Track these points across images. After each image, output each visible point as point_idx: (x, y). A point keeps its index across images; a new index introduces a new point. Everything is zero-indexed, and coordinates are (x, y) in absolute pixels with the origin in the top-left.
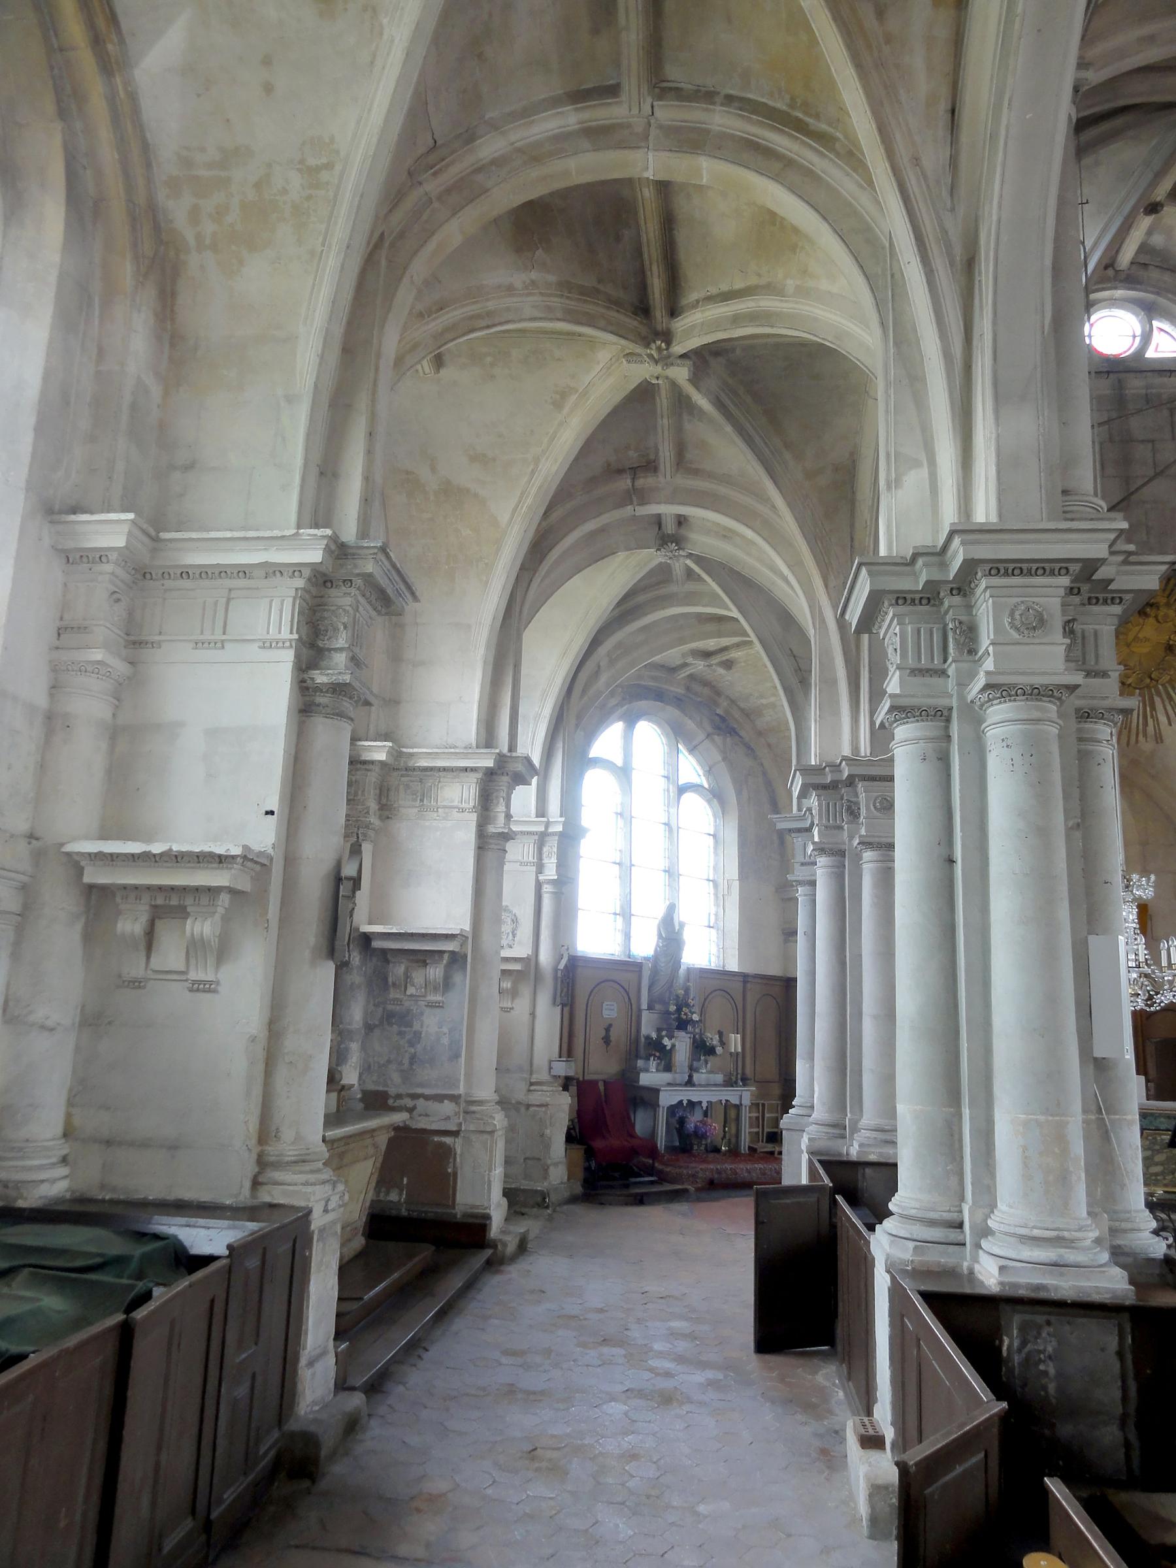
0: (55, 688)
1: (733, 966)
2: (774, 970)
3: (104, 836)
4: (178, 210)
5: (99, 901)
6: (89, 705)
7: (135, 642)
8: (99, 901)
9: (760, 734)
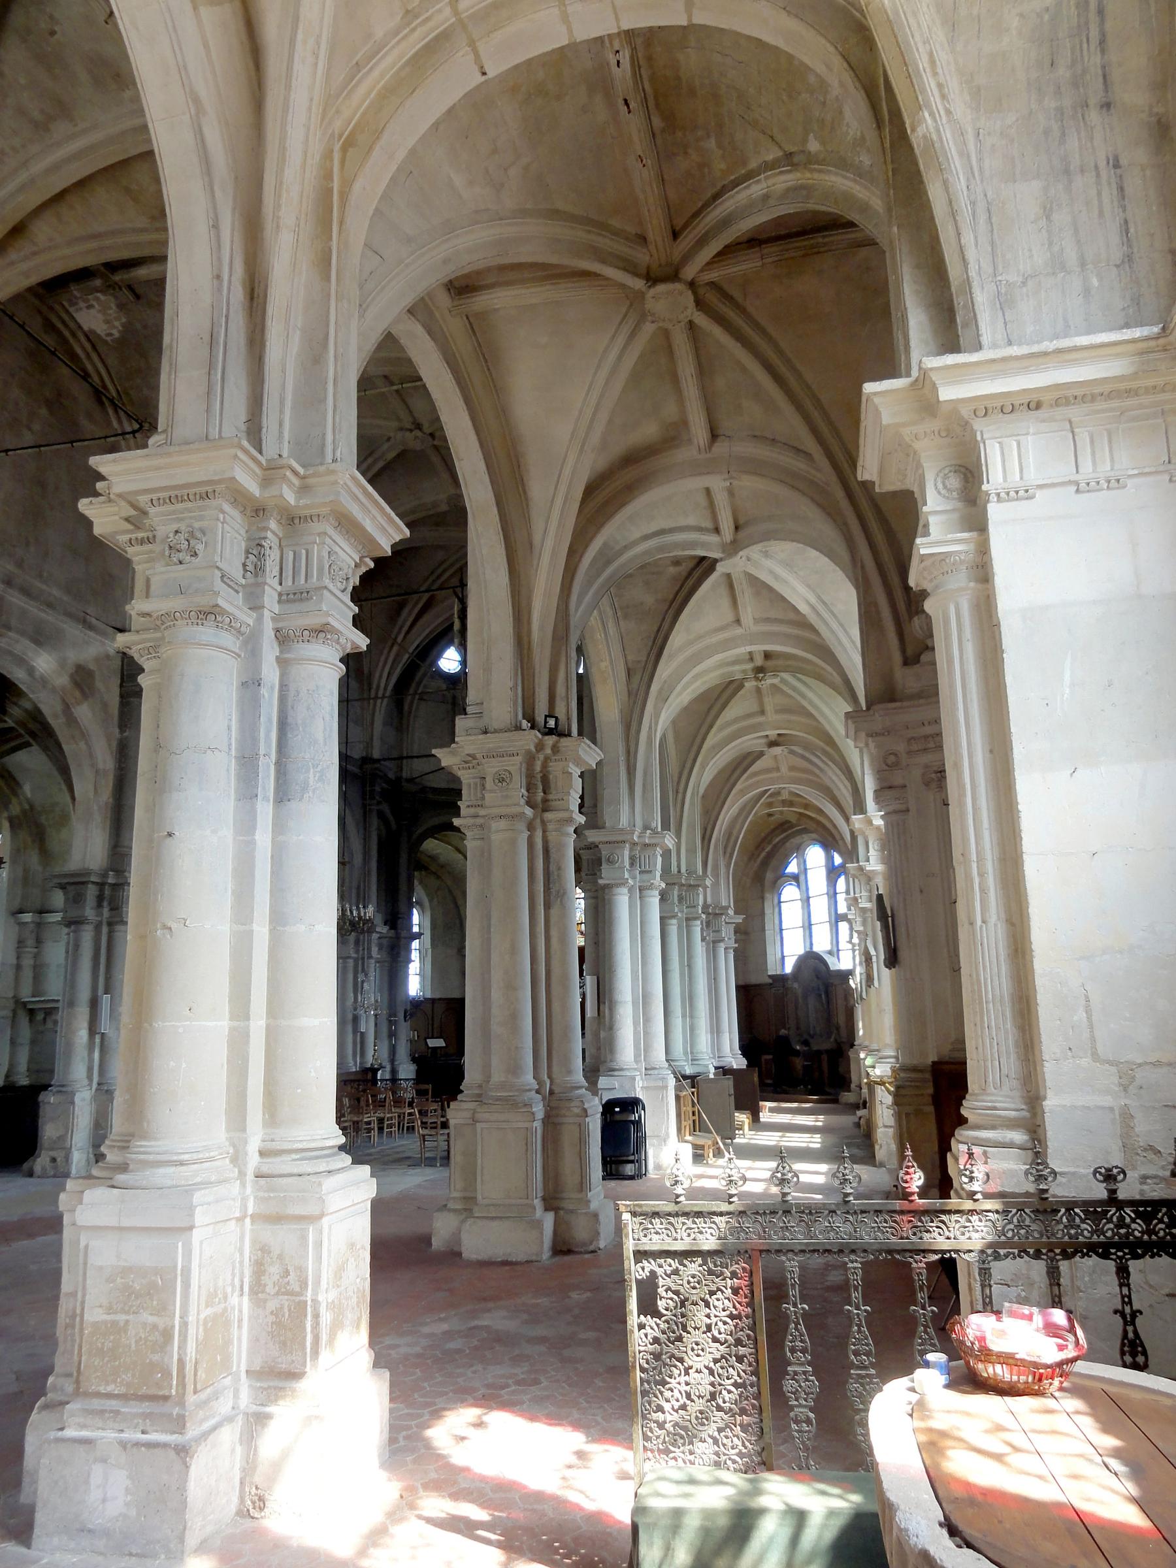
0: (18, 958)
1: (429, 995)
2: (456, 995)
3: (33, 996)
4: (43, 819)
5: (32, 1012)
6: (28, 962)
7: (39, 942)
8: (32, 1012)
9: (442, 867)
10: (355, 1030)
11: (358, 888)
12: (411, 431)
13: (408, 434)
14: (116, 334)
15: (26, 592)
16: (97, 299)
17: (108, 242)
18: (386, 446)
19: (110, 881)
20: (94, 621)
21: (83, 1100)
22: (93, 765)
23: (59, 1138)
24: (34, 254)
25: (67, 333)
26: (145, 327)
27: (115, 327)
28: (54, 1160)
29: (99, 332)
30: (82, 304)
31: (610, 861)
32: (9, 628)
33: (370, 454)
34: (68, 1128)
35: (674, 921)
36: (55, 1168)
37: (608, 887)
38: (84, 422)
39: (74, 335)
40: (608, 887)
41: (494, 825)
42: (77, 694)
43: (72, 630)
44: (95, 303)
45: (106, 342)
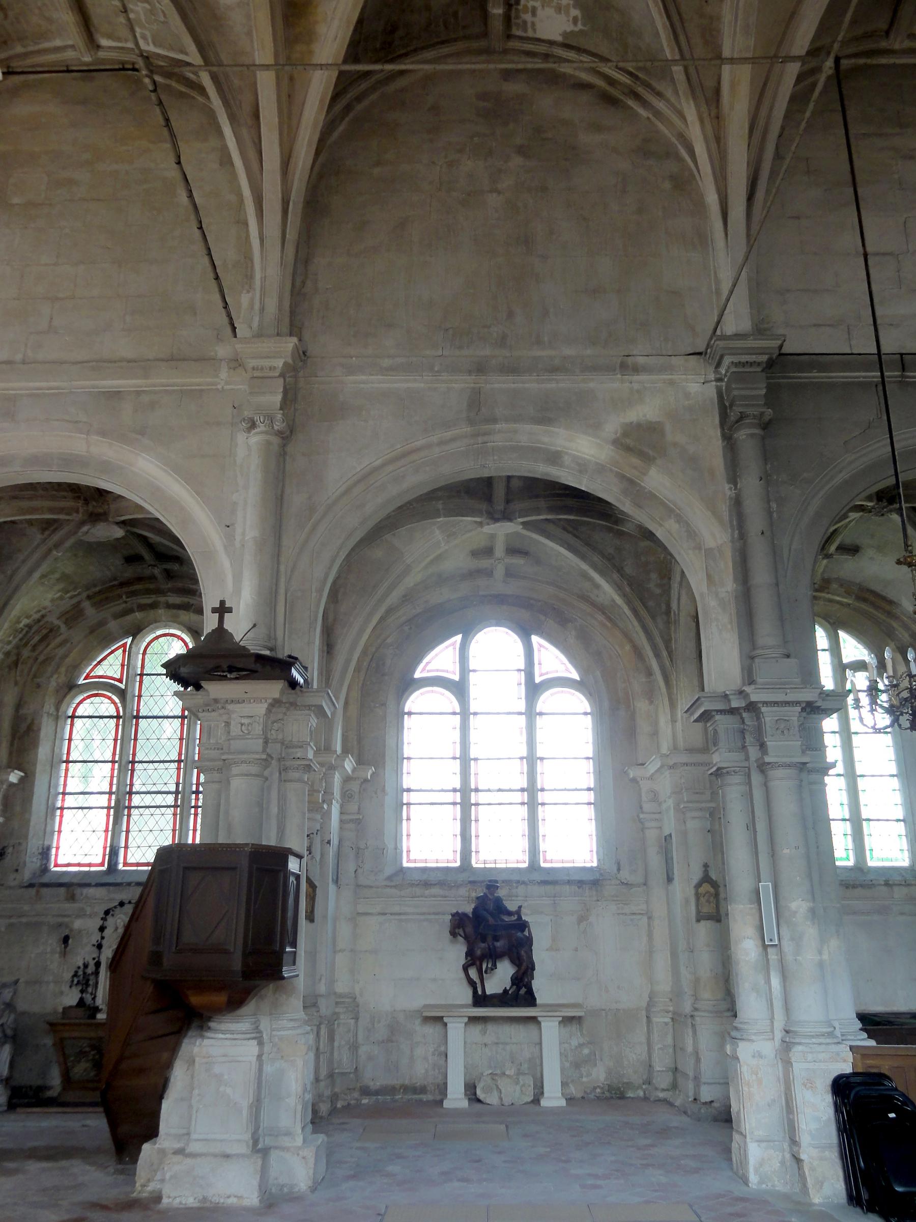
15: (511, 369)
20: (641, 360)
21: (759, 1055)
22: (698, 547)
29: (568, 30)
30: (528, 17)
32: (495, 421)
38: (586, 139)
39: (546, 57)
42: (635, 461)
43: (607, 386)
45: (581, 31)
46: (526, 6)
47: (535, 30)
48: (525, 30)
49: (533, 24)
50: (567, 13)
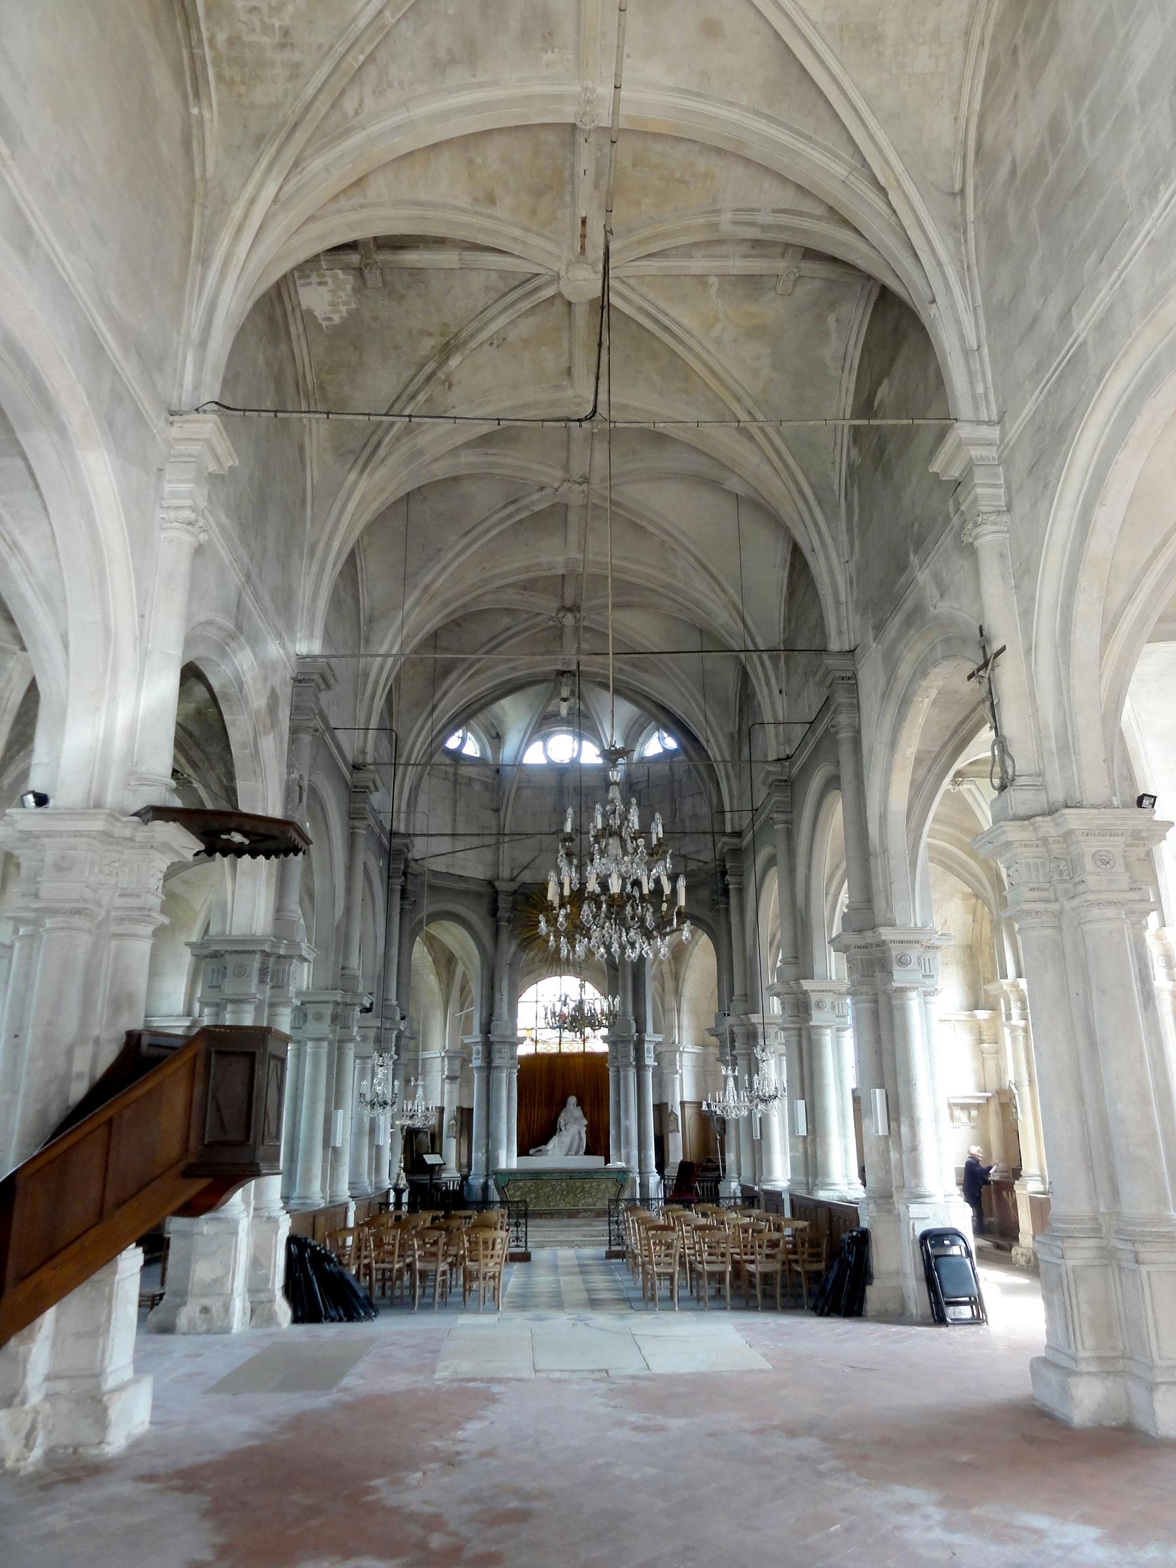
10: (371, 1144)
11: (379, 977)
12: (580, 484)
13: (577, 486)
14: (337, 319)
16: (335, 277)
17: (429, 213)
18: (535, 497)
19: (282, 952)
23: (216, 1281)
24: (361, 206)
25: (289, 308)
26: (375, 318)
27: (339, 312)
28: (205, 1310)
29: (316, 313)
31: (902, 962)
33: (513, 502)
34: (229, 1268)
35: (828, 1031)
36: (210, 1320)
37: (902, 991)
40: (902, 991)
41: (1096, 912)
44: (330, 281)
45: (319, 326)
46: (324, 276)
47: (304, 285)
48: (300, 278)
49: (310, 284)
50: (332, 312)
